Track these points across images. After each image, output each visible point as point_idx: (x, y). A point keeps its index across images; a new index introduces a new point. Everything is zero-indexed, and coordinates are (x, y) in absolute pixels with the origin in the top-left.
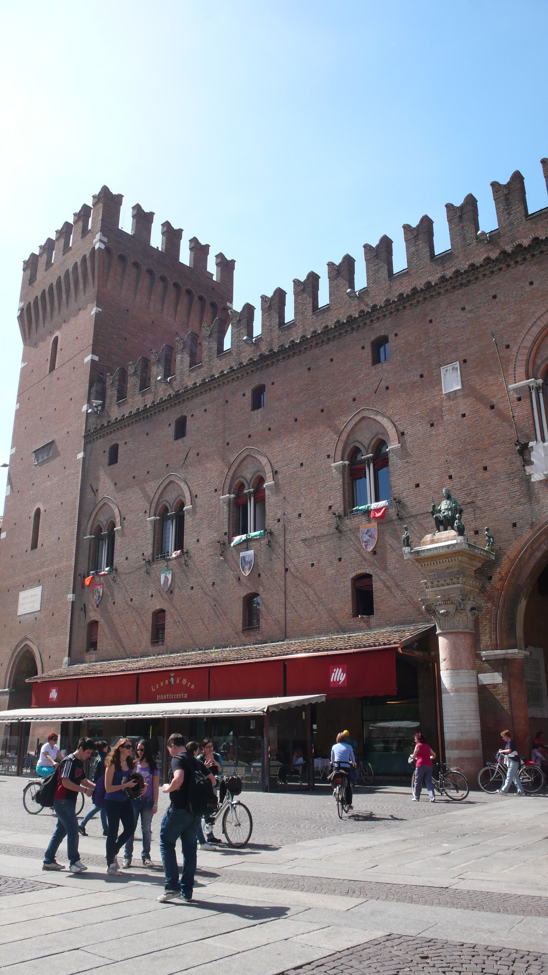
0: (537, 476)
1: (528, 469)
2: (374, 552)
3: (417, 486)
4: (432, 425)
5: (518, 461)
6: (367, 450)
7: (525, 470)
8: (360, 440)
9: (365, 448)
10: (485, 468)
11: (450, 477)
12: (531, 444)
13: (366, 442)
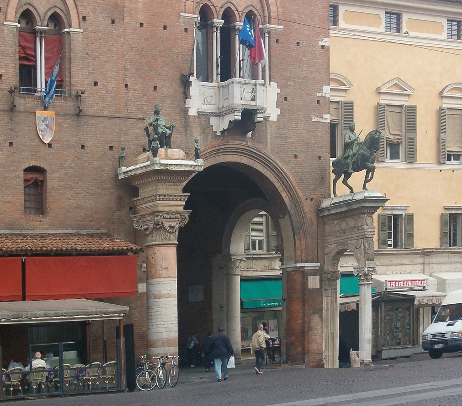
0: (192, 112)
1: (189, 103)
2: (50, 145)
3: (96, 84)
4: (113, 22)
5: (181, 90)
6: (42, 21)
7: (185, 102)
8: (35, 5)
9: (40, 18)
10: (155, 88)
11: (126, 86)
12: (192, 79)
13: (42, 10)
